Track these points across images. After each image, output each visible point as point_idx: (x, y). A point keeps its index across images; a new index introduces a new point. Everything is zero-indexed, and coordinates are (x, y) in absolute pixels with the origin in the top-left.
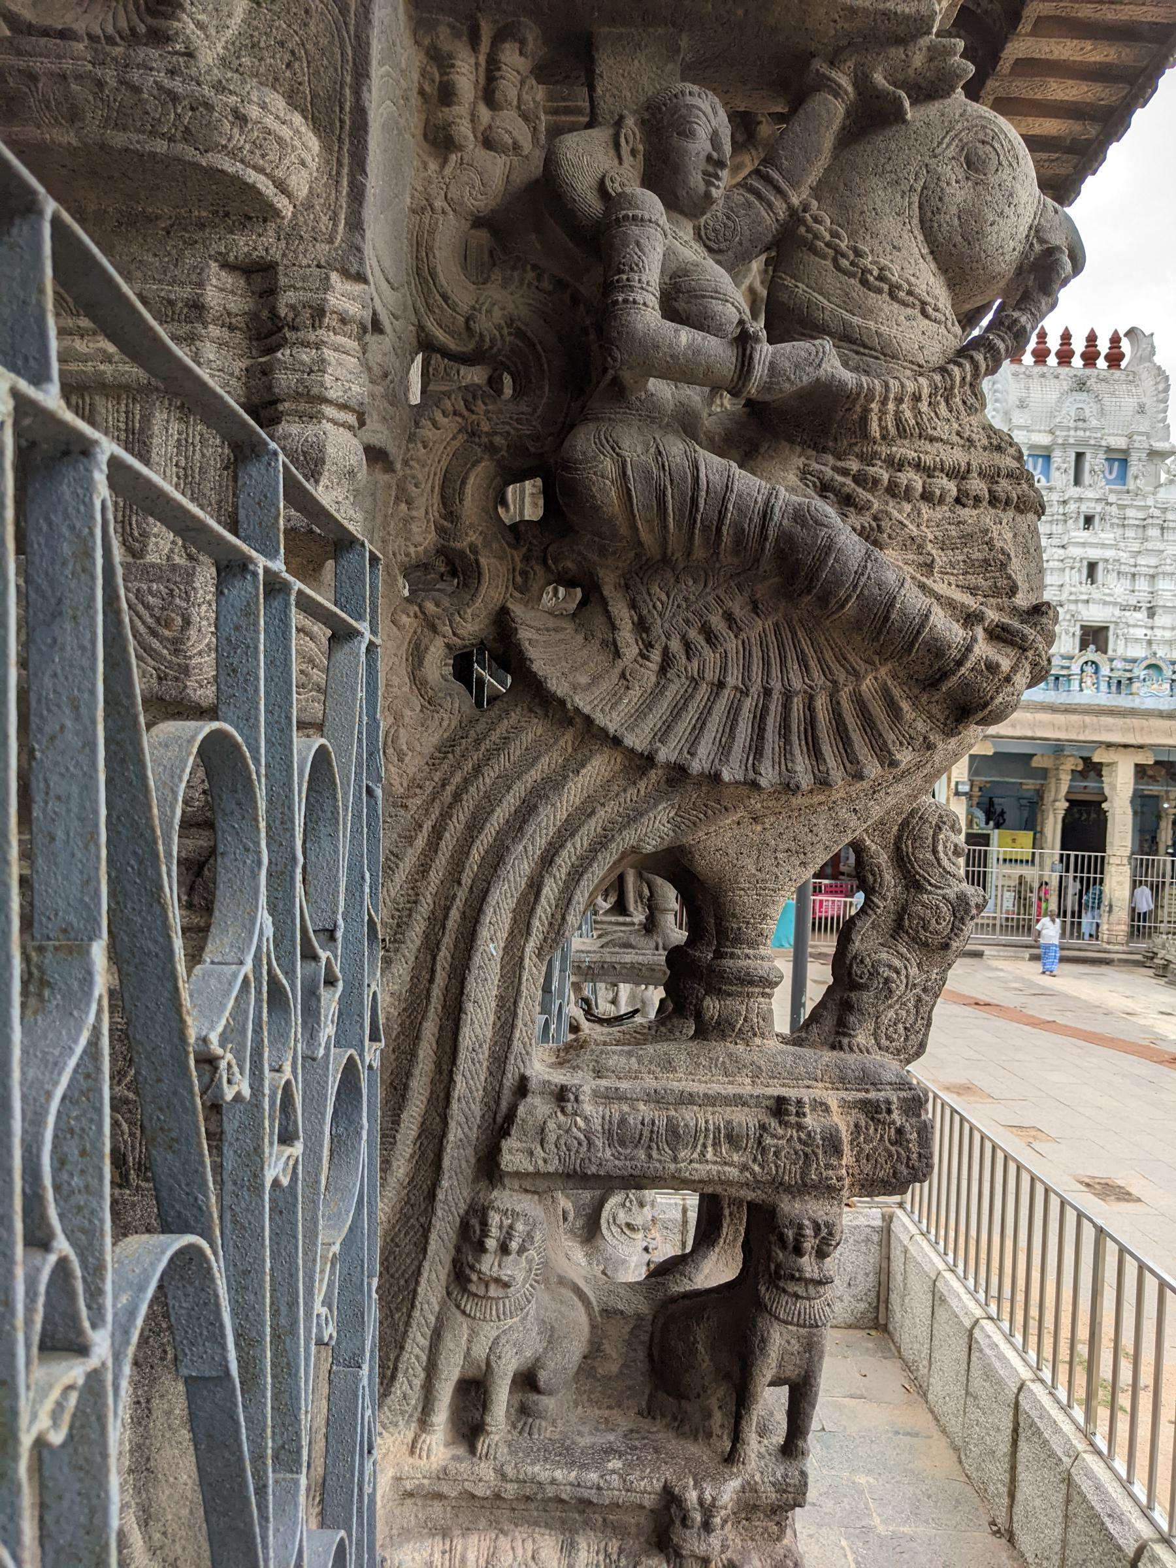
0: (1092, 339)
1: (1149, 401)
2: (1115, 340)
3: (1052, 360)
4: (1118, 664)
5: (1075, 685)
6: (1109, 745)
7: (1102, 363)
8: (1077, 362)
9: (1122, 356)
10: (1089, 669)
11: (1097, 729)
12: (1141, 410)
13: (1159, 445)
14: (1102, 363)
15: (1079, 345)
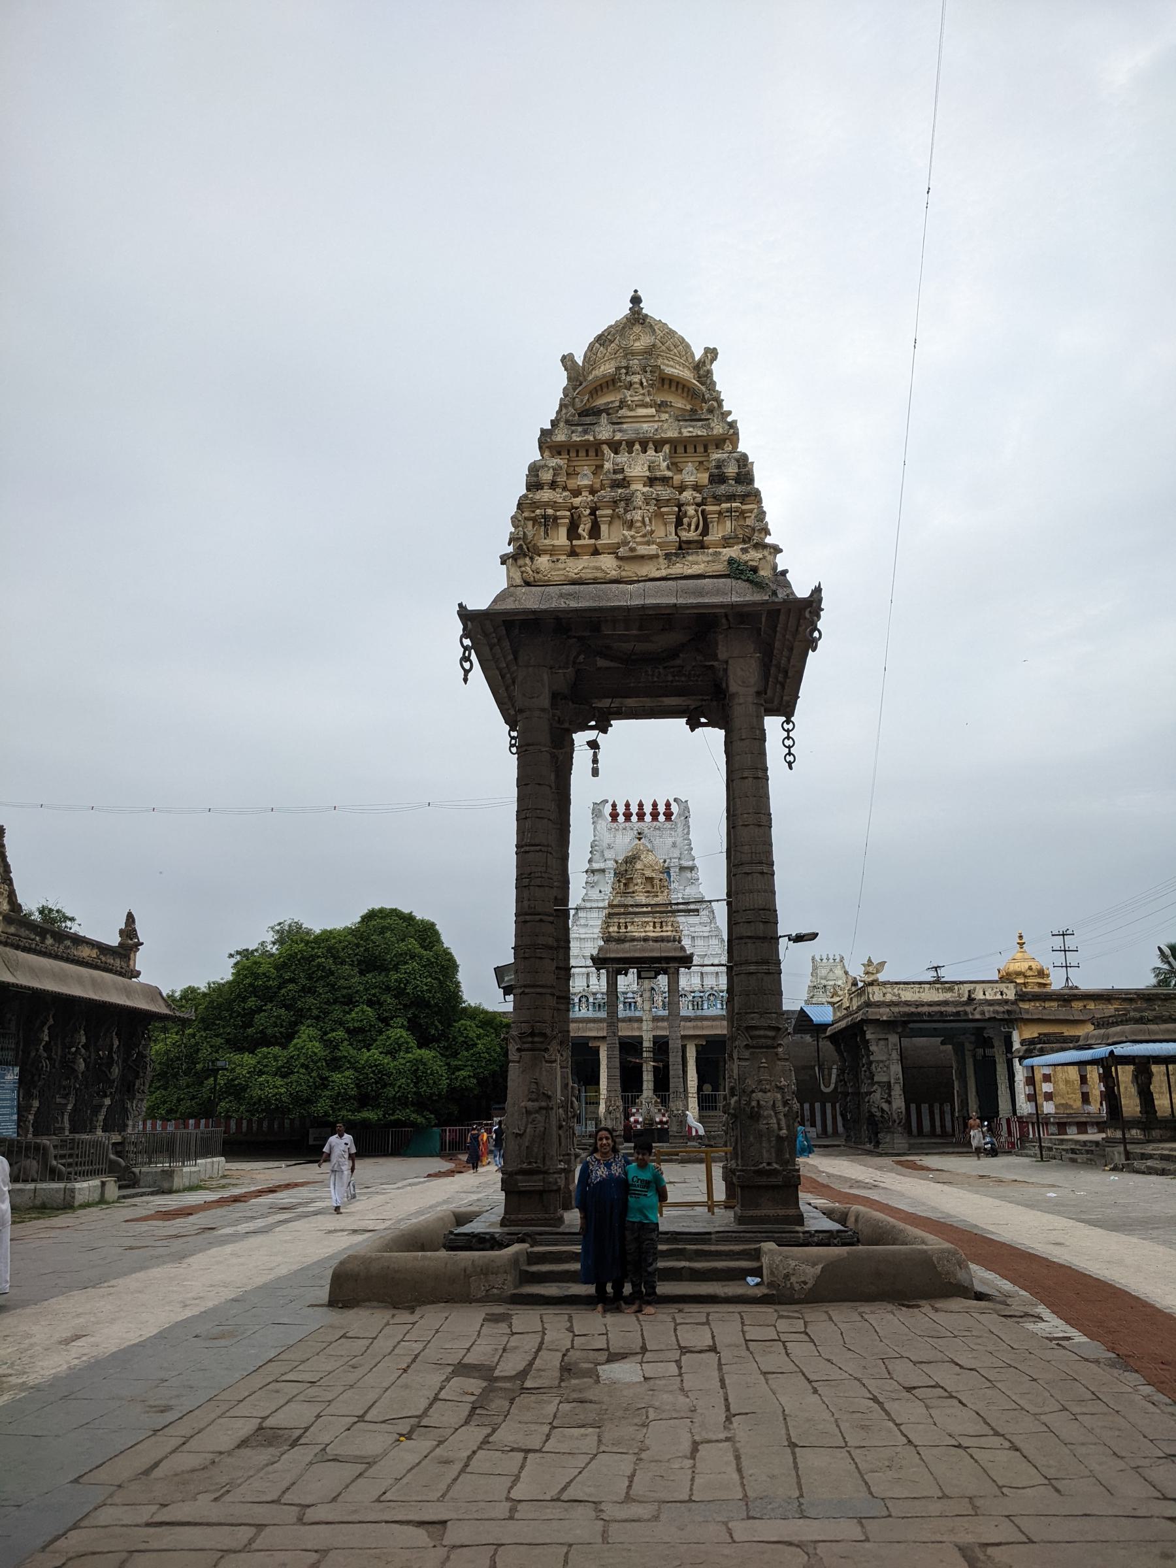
0: (655, 805)
1: (679, 840)
2: (668, 805)
3: (634, 818)
4: (599, 996)
5: (577, 1008)
6: (595, 1038)
7: (662, 818)
8: (648, 818)
9: (672, 814)
10: (584, 1000)
11: (585, 1030)
12: (674, 845)
13: (685, 863)
14: (662, 818)
15: (648, 809)
